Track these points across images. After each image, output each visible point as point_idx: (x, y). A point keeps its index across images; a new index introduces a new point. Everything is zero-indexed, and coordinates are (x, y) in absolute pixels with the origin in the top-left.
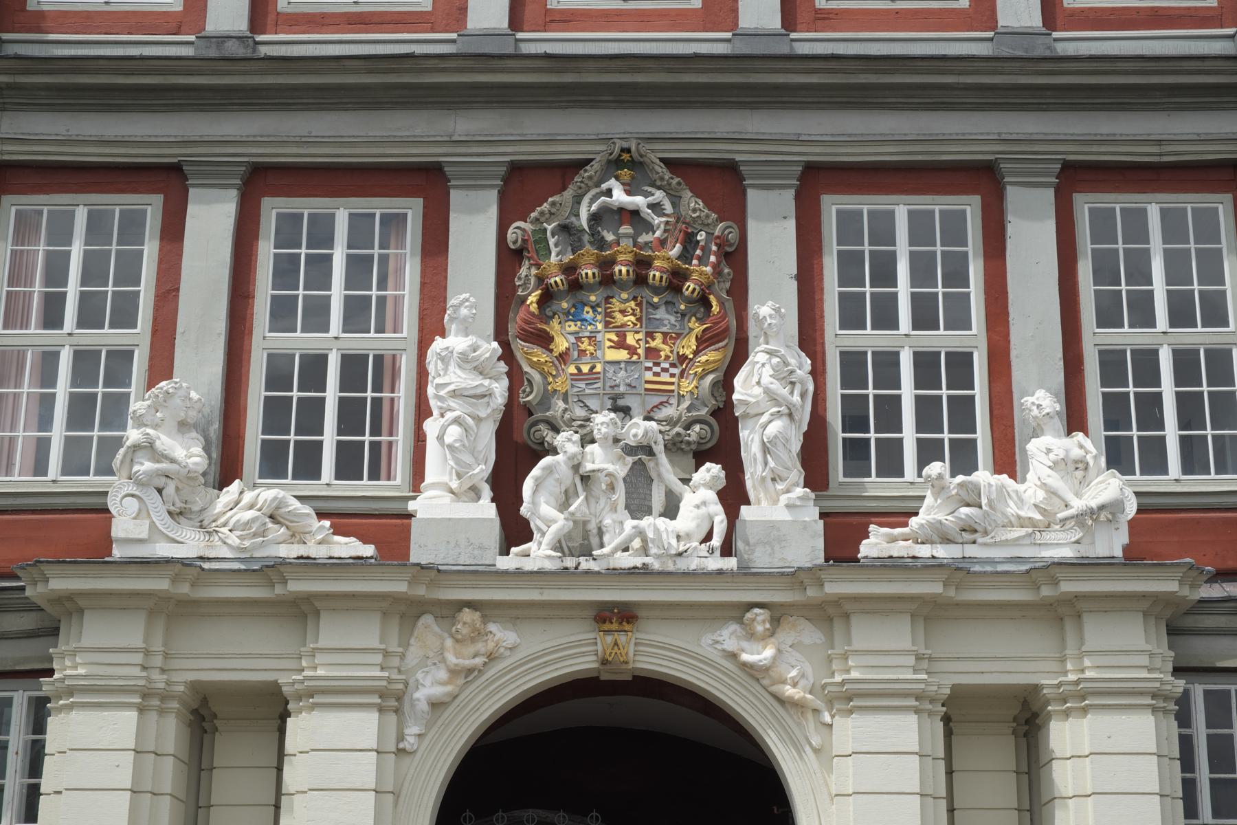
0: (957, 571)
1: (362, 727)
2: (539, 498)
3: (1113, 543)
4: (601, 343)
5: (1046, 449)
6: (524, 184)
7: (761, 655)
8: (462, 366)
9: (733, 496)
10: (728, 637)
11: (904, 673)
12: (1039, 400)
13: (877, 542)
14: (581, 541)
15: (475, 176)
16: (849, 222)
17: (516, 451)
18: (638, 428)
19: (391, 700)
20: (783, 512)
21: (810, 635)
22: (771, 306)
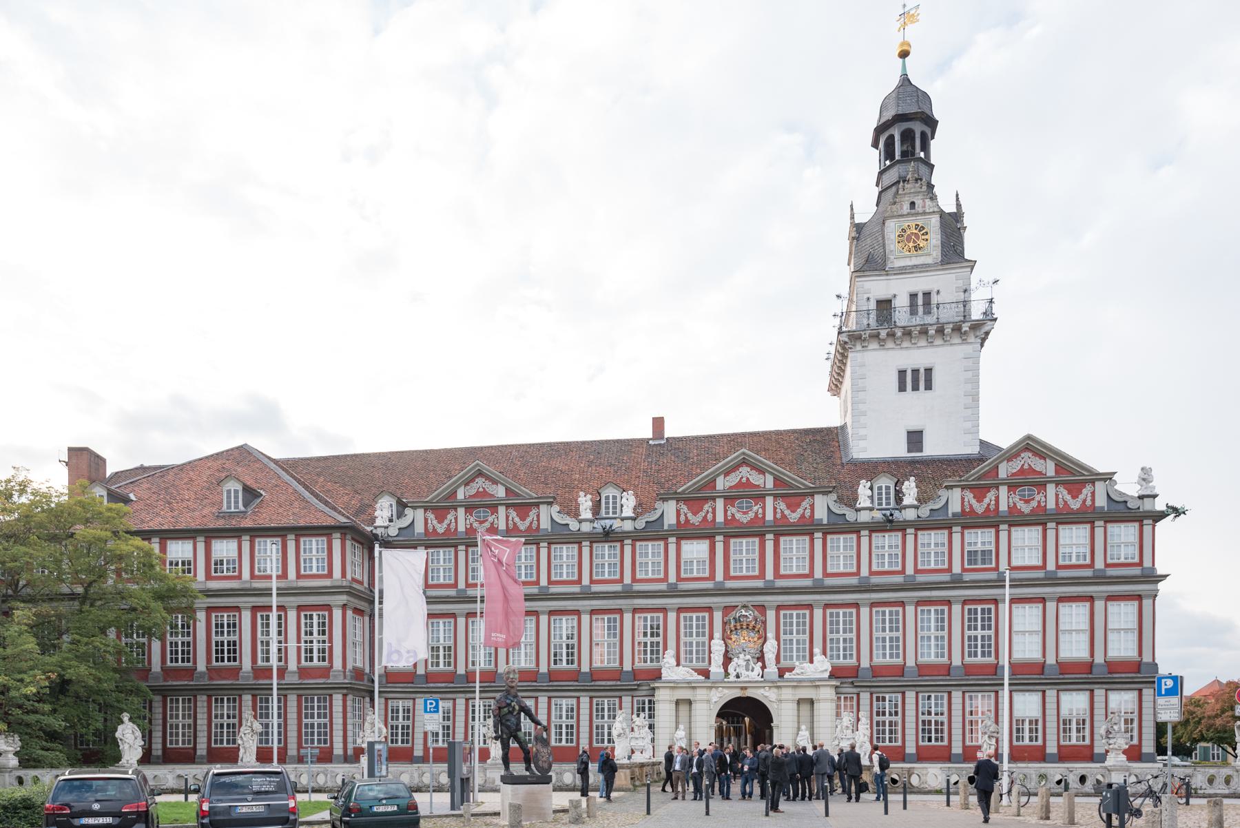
0: (800, 681)
1: (705, 706)
2: (731, 669)
3: (827, 675)
4: (744, 640)
5: (818, 657)
6: (727, 610)
7: (767, 694)
8: (718, 646)
9: (764, 667)
10: (762, 691)
11: (790, 697)
12: (817, 650)
13: (787, 675)
14: (738, 676)
15: (718, 608)
16: (785, 615)
17: (727, 660)
18: (748, 657)
19: (708, 701)
20: (772, 669)
21: (775, 690)
22: (771, 635)
